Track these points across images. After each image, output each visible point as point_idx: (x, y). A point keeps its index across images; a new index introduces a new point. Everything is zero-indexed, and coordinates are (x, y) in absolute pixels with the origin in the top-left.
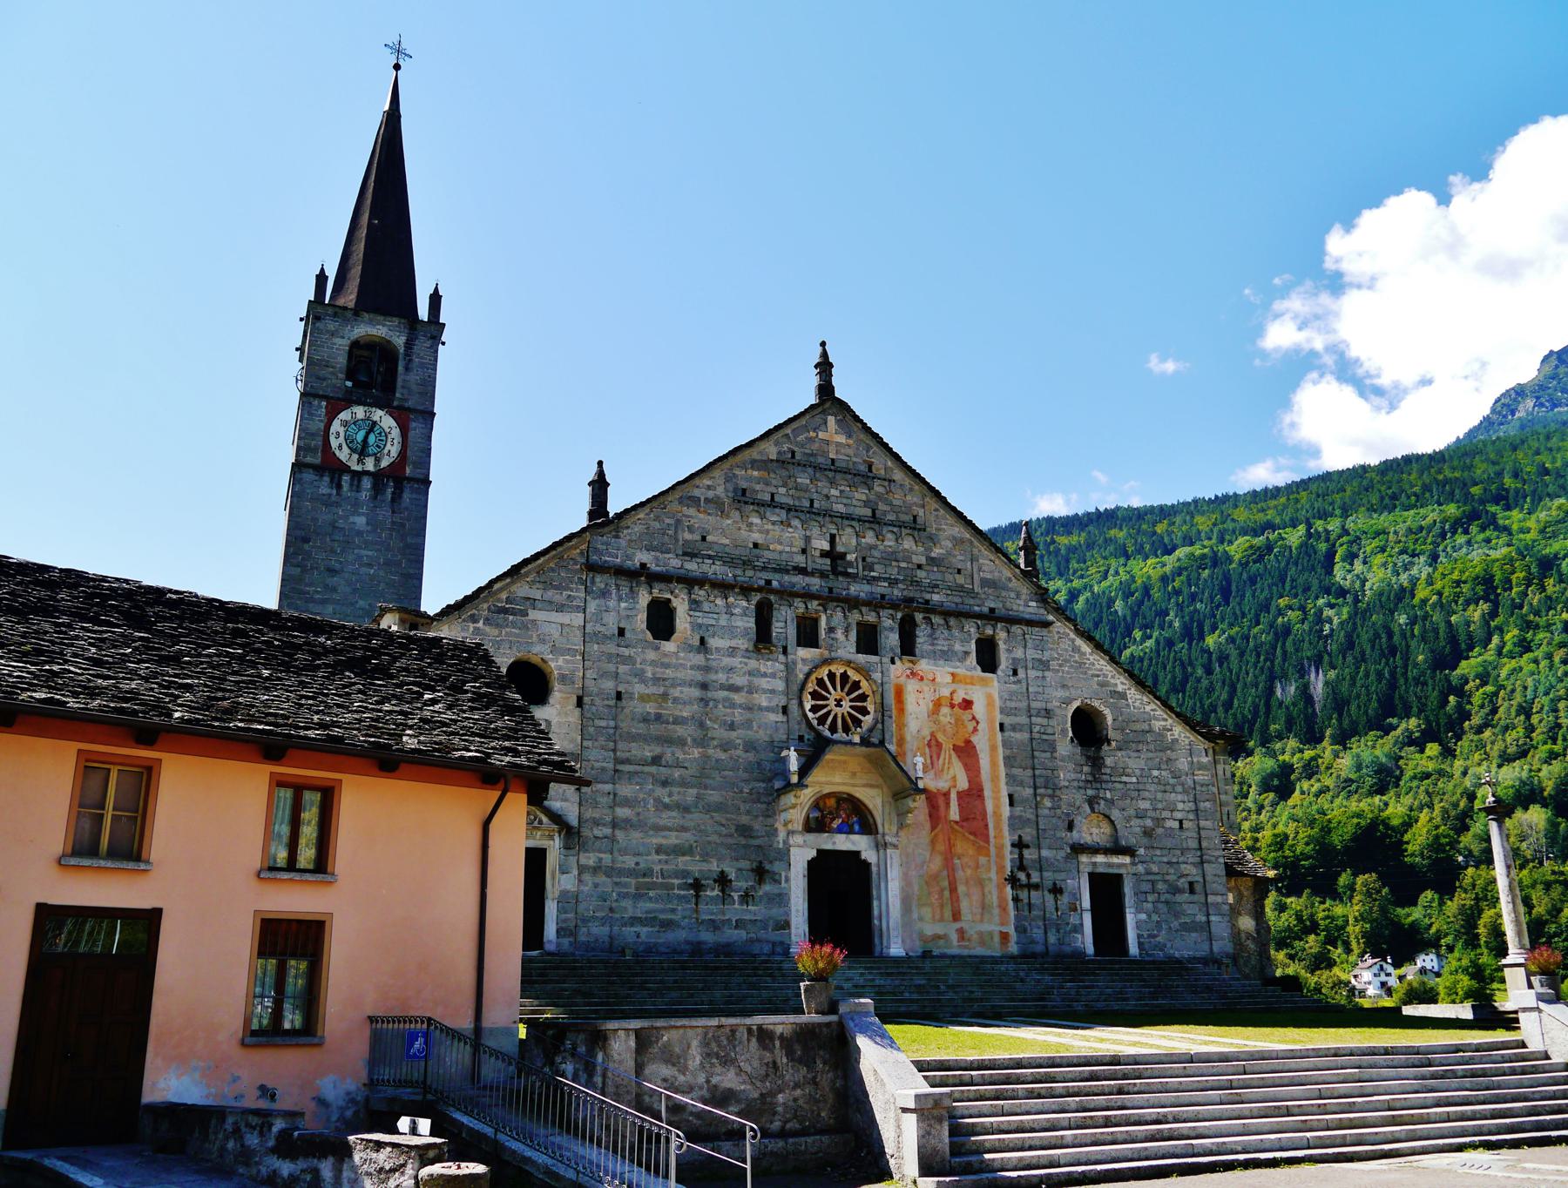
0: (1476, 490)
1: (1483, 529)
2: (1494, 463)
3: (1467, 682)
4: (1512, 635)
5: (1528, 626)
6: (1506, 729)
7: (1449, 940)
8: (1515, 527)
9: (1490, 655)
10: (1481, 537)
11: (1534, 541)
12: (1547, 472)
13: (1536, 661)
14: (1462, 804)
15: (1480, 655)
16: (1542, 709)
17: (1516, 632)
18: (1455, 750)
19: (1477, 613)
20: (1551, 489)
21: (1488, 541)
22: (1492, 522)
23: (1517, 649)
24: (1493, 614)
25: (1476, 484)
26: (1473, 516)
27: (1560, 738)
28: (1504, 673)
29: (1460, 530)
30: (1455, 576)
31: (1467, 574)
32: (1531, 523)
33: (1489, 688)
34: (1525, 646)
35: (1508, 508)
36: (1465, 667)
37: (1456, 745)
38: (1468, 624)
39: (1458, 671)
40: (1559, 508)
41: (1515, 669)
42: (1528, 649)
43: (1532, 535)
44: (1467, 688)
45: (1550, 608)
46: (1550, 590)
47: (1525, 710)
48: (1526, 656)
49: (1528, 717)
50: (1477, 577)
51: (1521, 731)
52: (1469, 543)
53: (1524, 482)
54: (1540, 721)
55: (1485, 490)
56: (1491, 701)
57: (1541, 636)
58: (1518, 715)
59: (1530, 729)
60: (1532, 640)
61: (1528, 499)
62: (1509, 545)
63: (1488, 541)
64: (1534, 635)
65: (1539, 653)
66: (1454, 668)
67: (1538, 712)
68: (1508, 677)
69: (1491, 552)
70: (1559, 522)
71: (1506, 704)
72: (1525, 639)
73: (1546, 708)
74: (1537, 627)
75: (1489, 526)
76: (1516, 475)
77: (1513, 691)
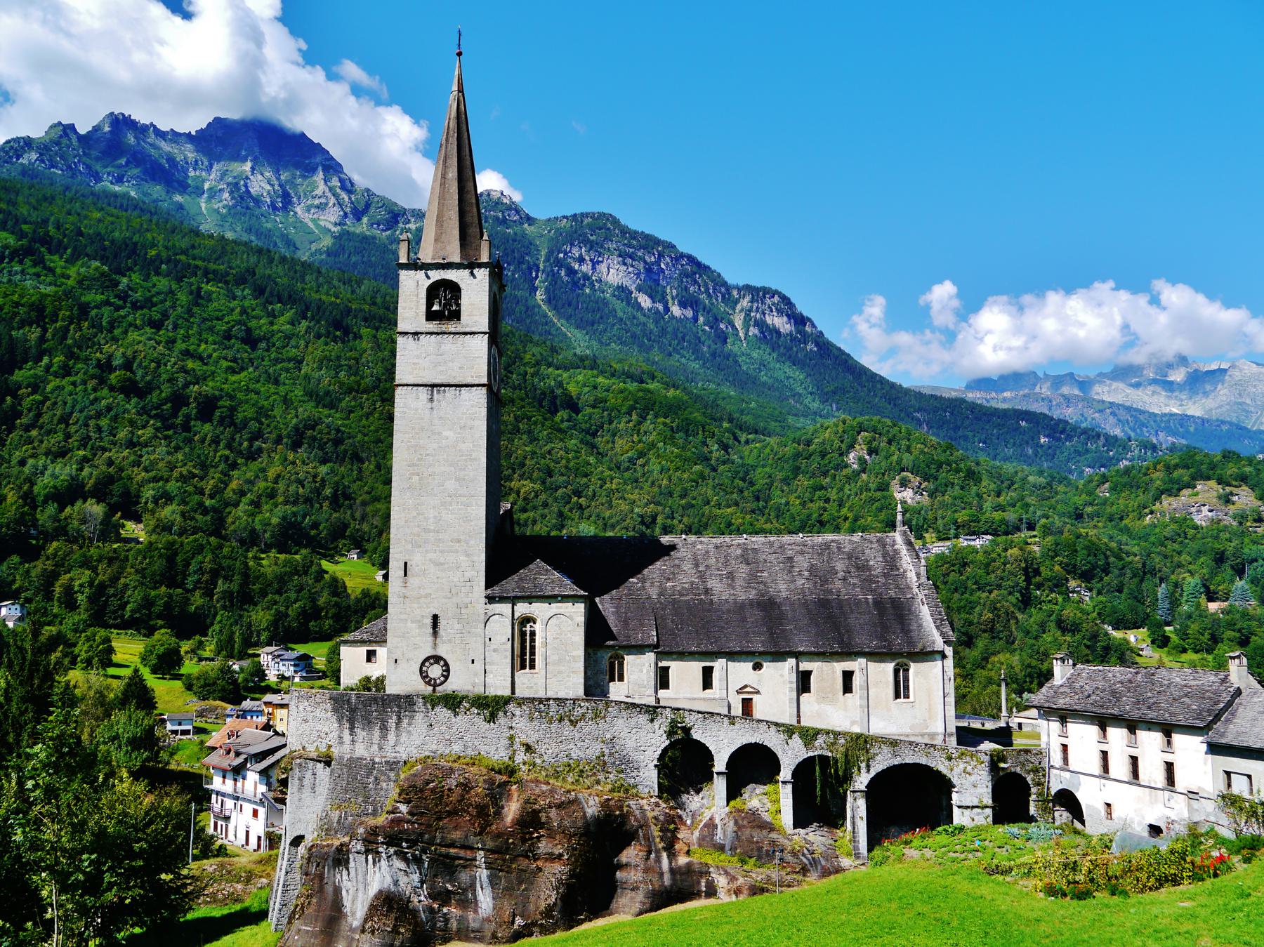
0: (25, 227)
1: (35, 264)
2: (35, 208)
3: (20, 388)
4: (58, 359)
5: (71, 355)
6: (49, 432)
7: (29, 594)
8: (58, 271)
9: (39, 371)
10: (32, 270)
11: (73, 288)
12: (80, 233)
13: (74, 384)
14: (25, 488)
15: (30, 370)
16: (77, 422)
17: (62, 358)
18: (6, 440)
19: (34, 334)
20: (89, 250)
21: (38, 275)
22: (39, 262)
23: (61, 371)
24: (42, 339)
25: (26, 223)
26: (28, 251)
27: (89, 446)
28: (49, 387)
29: (16, 259)
30: (15, 298)
31: (25, 299)
32: (72, 271)
33: (38, 397)
34: (66, 371)
35: (50, 252)
36: (18, 376)
37: (7, 436)
38: (26, 341)
39: (14, 378)
40: (96, 269)
41: (59, 387)
42: (69, 374)
43: (71, 282)
44: (20, 392)
45: (88, 347)
46: (85, 331)
47: (65, 420)
48: (67, 379)
49: (67, 425)
50: (33, 304)
51: (60, 437)
52: (23, 272)
53: (65, 236)
54: (77, 431)
55: (34, 231)
56: (38, 407)
57: (80, 366)
58: (60, 422)
59: (68, 436)
60: (73, 367)
61: (69, 251)
62: (56, 285)
63: (38, 275)
64: (75, 364)
65: (78, 378)
66: (12, 374)
67: (73, 424)
68: (52, 392)
69: (42, 286)
70: (94, 279)
71: (51, 413)
72: (67, 365)
73: (80, 422)
74: (78, 358)
75: (39, 263)
76: (58, 228)
77: (55, 403)
